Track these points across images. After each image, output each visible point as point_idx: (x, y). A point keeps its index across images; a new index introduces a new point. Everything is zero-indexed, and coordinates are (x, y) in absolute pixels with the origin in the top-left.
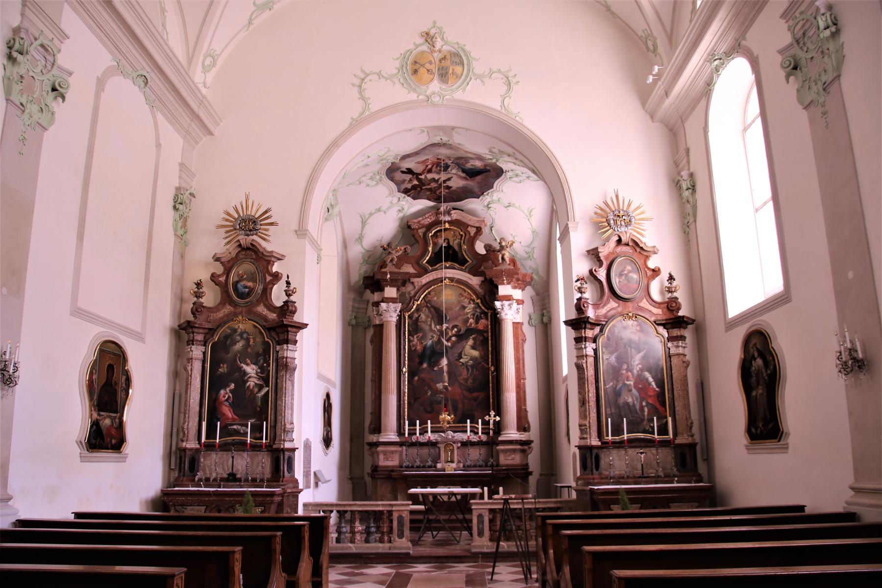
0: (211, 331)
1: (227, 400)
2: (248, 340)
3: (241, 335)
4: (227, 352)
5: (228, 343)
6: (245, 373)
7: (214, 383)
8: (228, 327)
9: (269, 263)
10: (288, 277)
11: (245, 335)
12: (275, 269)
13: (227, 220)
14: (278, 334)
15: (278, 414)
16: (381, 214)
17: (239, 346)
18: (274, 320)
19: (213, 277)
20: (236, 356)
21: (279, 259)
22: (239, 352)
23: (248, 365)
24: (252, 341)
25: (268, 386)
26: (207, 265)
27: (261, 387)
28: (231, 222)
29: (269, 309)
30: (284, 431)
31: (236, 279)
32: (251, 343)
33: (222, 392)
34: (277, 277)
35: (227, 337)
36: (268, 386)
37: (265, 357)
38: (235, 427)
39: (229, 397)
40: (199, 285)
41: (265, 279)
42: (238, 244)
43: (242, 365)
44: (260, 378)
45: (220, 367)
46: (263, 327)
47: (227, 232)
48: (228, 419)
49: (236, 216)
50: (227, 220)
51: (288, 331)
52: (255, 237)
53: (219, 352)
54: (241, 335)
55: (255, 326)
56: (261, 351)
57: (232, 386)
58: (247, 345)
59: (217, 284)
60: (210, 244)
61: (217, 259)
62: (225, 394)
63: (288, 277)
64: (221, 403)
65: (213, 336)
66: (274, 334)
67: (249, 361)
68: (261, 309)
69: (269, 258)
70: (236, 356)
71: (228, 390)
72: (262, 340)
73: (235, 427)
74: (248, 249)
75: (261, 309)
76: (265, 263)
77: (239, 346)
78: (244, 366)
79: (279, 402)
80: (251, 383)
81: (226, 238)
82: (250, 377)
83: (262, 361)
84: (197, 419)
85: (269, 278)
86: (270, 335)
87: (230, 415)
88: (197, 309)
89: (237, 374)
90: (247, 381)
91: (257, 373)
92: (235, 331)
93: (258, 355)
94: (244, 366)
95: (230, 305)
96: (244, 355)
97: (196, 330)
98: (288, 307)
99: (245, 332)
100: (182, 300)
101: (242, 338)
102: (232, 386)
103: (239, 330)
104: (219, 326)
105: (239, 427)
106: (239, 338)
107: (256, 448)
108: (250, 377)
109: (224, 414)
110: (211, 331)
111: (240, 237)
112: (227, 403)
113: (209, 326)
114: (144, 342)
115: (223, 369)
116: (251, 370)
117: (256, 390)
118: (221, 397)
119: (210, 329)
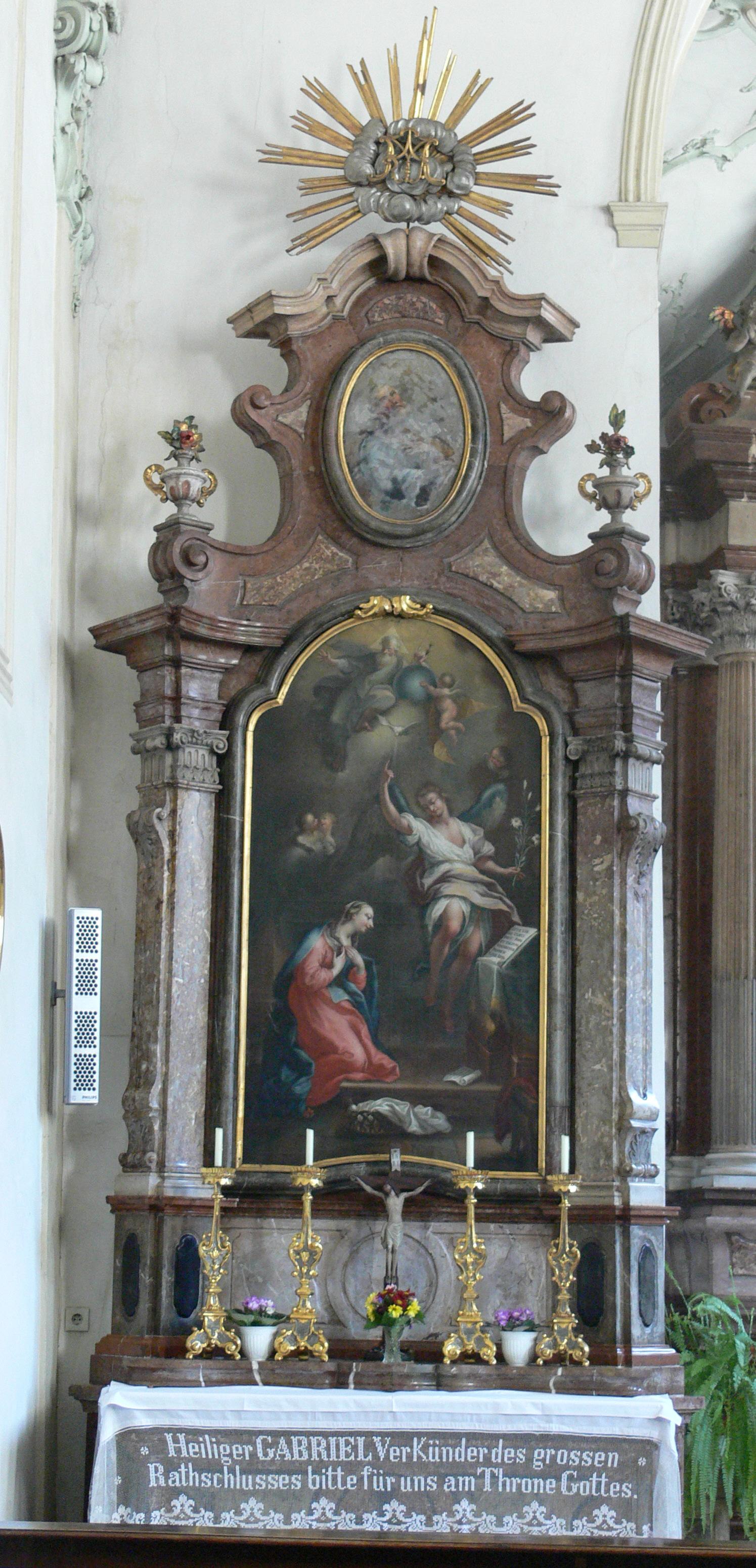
0: (264, 658)
1: (341, 981)
2: (430, 705)
3: (398, 680)
4: (333, 755)
5: (336, 717)
6: (422, 860)
7: (286, 895)
8: (333, 645)
9: (513, 351)
10: (617, 419)
11: (416, 684)
12: (532, 383)
13: (314, 129)
14: (570, 681)
15: (585, 1047)
16: (708, 163)
17: (389, 733)
18: (546, 615)
19: (246, 413)
20: (376, 778)
21: (559, 338)
22: (389, 759)
23: (433, 819)
24: (449, 709)
25: (532, 920)
26: (189, 345)
27: (499, 926)
28: (336, 140)
29: (516, 567)
30: (623, 1127)
31: (363, 416)
32: (447, 718)
33: (317, 942)
34: (551, 414)
35: (331, 690)
36: (532, 920)
37: (512, 785)
38: (382, 1106)
39: (350, 967)
40: (180, 440)
41: (523, 434)
42: (368, 256)
43: (409, 819)
44: (493, 883)
45: (302, 828)
46: (508, 648)
47: (309, 187)
48: (347, 1067)
49: (364, 118)
50: (314, 129)
51: (627, 672)
52: (437, 228)
53: (300, 749)
54: (398, 680)
55: (462, 643)
56: (495, 757)
57: (365, 916)
58: (430, 727)
59: (264, 441)
60: (222, 249)
61: (263, 323)
62: (327, 952)
63: (617, 419)
64: (315, 994)
65: (261, 680)
66: (552, 683)
67: (439, 805)
68: (485, 563)
69: (515, 330)
70: (376, 778)
71: (344, 932)
72: (496, 707)
73: (382, 1106)
74: (414, 280)
75: (485, 563)
76: (493, 353)
77: (389, 733)
78: (419, 827)
79: (588, 997)
80: (453, 906)
81: (304, 213)
82: (446, 878)
83: (500, 806)
84: (200, 1067)
85: (514, 423)
86: (540, 690)
87: (358, 1053)
88: (175, 553)
89: (382, 865)
90: (433, 896)
91: (479, 861)
92: (368, 661)
93: (481, 776)
94: (419, 827)
95: (336, 541)
96: (413, 777)
97: (189, 651)
98: (621, 555)
99: (417, 668)
100: (81, 513)
101: (402, 695)
102: (365, 916)
103: (389, 661)
104: (294, 637)
105: (402, 1108)
106: (385, 695)
107: (500, 1207)
108: (446, 878)
109: (325, 1048)
110: (264, 658)
111: (374, 223)
112: (339, 996)
113: (249, 632)
114: (11, 704)
115: (319, 836)
116: (450, 843)
117: (477, 937)
118: (313, 964)
119: (248, 649)
